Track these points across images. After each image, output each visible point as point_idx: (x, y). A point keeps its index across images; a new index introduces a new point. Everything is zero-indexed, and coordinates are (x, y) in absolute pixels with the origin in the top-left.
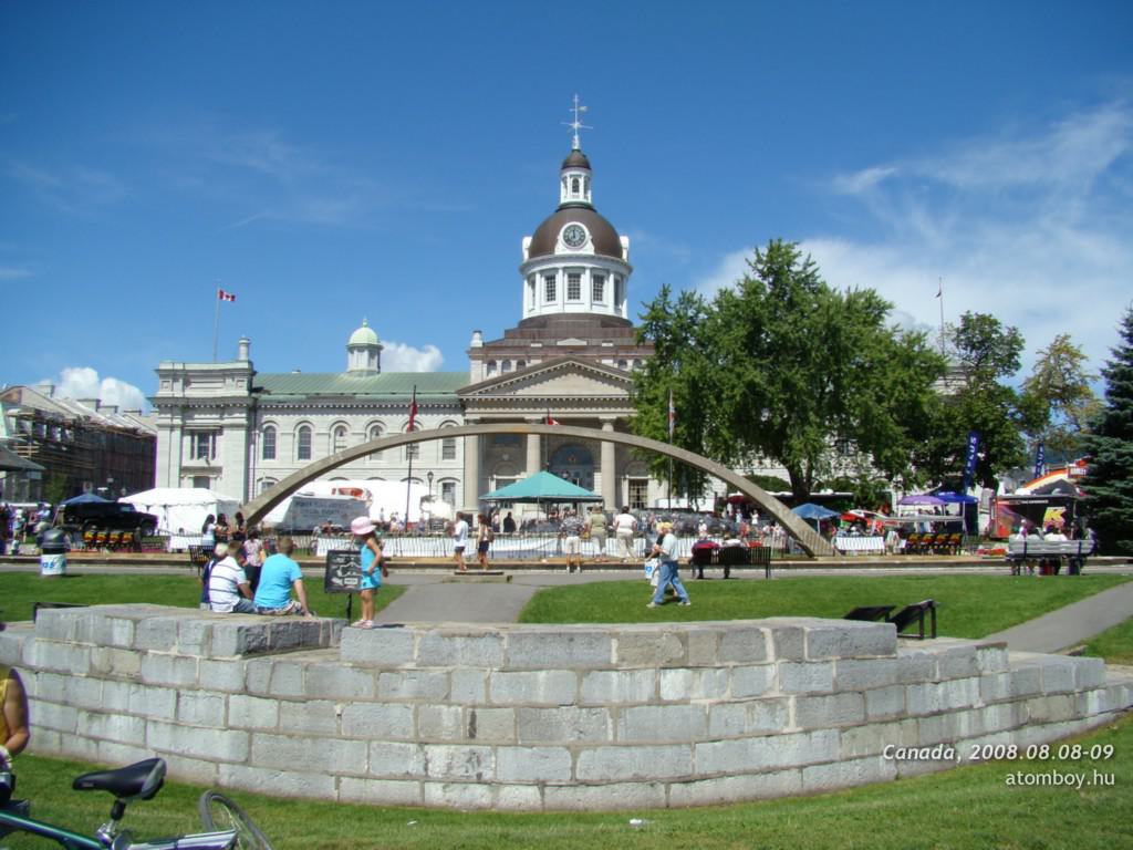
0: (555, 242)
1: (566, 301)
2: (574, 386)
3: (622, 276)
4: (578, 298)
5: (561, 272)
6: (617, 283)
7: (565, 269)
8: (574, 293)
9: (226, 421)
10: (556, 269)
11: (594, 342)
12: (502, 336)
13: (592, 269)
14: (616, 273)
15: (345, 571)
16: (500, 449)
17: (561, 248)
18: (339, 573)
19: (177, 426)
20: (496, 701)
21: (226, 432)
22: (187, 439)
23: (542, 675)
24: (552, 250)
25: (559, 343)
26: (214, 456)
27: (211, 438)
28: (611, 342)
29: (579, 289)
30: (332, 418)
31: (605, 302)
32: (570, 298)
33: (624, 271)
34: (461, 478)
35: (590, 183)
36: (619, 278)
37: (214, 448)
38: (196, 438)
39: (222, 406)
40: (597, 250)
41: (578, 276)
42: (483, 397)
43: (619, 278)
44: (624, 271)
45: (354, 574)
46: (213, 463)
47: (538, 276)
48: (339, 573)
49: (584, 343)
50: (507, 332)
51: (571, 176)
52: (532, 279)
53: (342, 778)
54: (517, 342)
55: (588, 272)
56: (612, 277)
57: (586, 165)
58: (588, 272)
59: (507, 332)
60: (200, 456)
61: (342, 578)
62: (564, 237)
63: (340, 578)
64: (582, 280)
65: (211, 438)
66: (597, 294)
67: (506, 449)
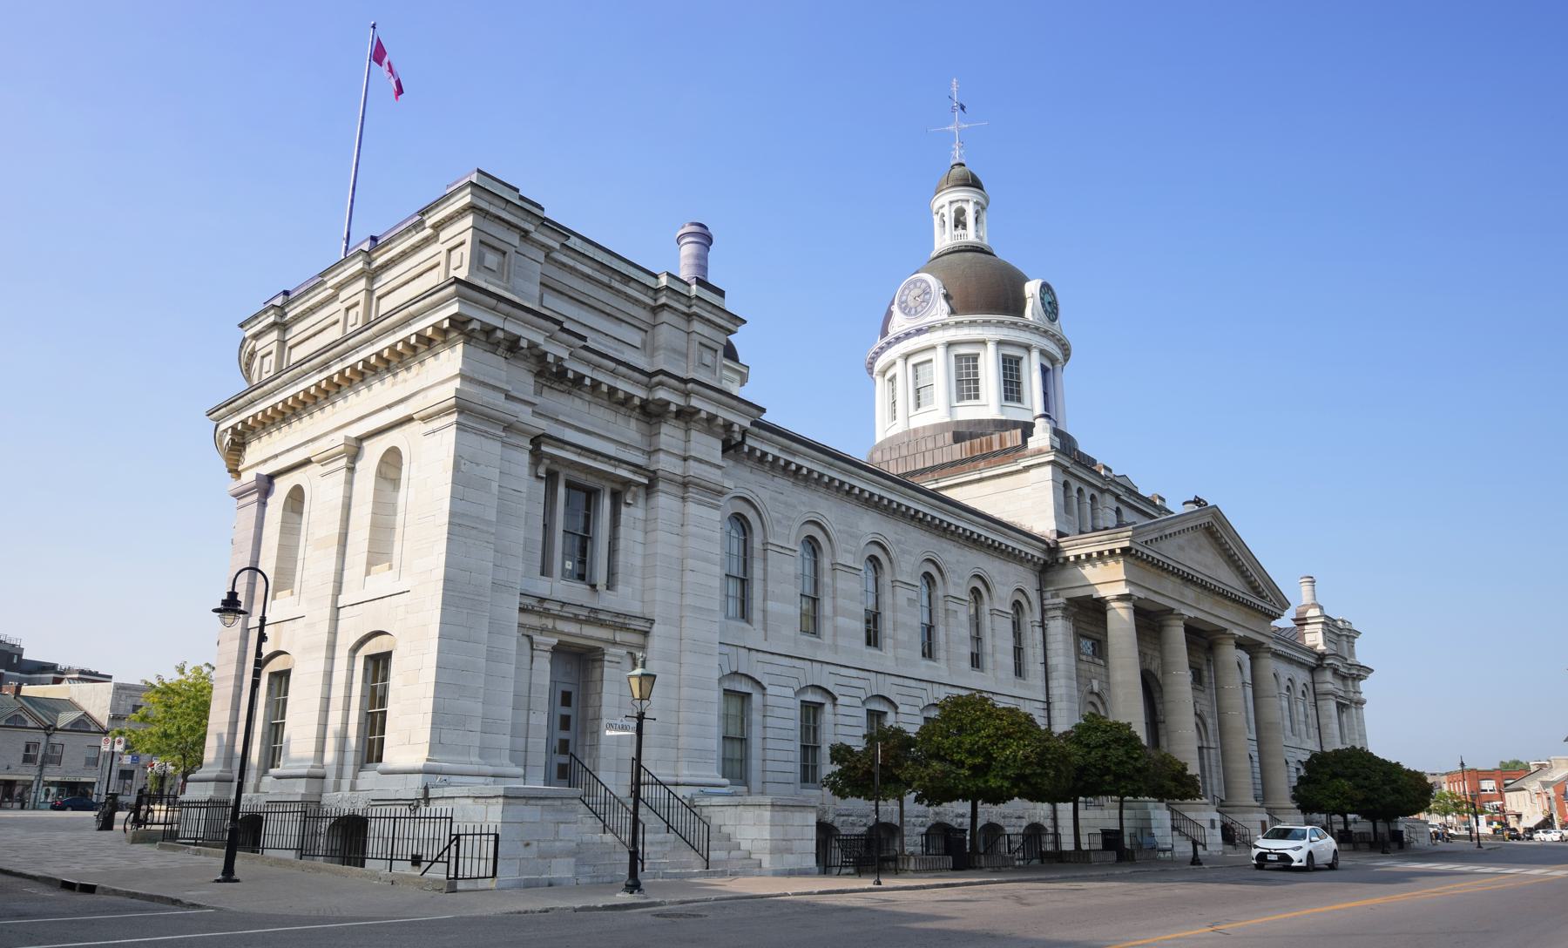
3: (1053, 360)
4: (977, 397)
5: (941, 351)
6: (1044, 370)
13: (1000, 343)
14: (1043, 353)
29: (976, 381)
31: (1027, 404)
35: (984, 217)
36: (1048, 365)
41: (975, 357)
43: (1048, 365)
47: (898, 369)
52: (889, 375)
57: (973, 183)
58: (991, 347)
64: (981, 361)
66: (1012, 389)
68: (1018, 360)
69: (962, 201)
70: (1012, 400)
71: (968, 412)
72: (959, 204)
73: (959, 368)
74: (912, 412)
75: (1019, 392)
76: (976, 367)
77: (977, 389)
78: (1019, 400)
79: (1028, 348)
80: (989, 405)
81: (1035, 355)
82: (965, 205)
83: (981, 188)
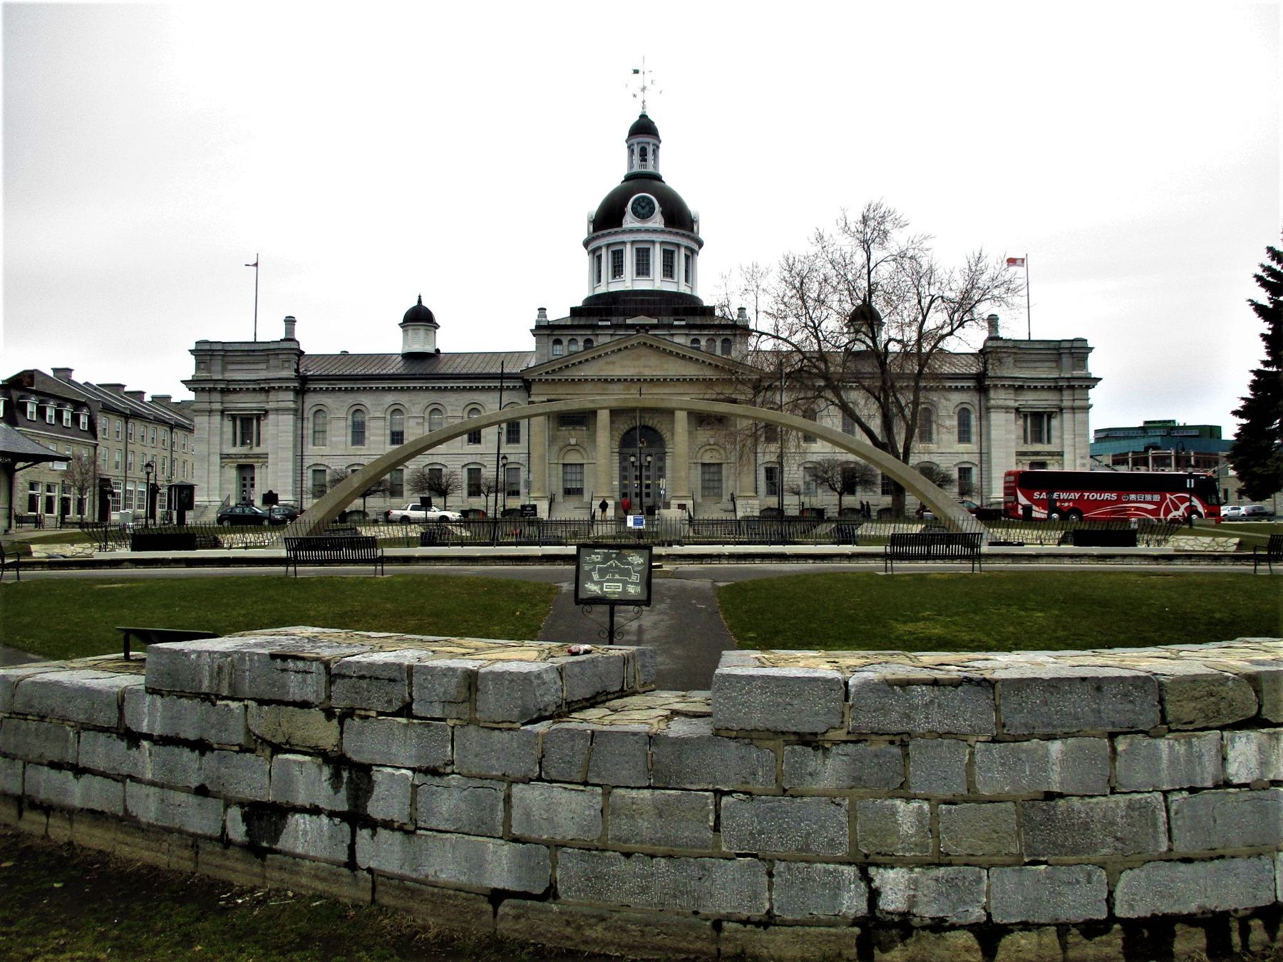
0: (623, 214)
1: (635, 278)
2: (645, 366)
4: (648, 274)
6: (687, 257)
7: (633, 242)
8: (643, 268)
9: (271, 405)
10: (624, 243)
11: (666, 320)
12: (568, 314)
13: (662, 243)
14: (687, 248)
15: (603, 573)
16: (567, 432)
17: (630, 221)
18: (596, 577)
19: (216, 411)
20: (985, 792)
21: (271, 417)
22: (228, 425)
23: (1056, 747)
24: (620, 225)
25: (629, 321)
26: (258, 444)
27: (255, 422)
28: (684, 320)
29: (648, 264)
30: (390, 399)
32: (638, 274)
33: (695, 247)
34: (526, 463)
36: (689, 254)
37: (259, 434)
38: (238, 423)
39: (264, 389)
40: (666, 224)
42: (550, 377)
43: (689, 254)
44: (695, 247)
45: (617, 577)
46: (256, 450)
47: (604, 251)
48: (596, 577)
49: (655, 321)
50: (572, 309)
51: (638, 143)
52: (598, 254)
53: (725, 924)
54: (583, 322)
55: (658, 246)
56: (683, 251)
58: (658, 246)
59: (572, 309)
60: (243, 443)
61: (600, 583)
62: (632, 209)
63: (596, 583)
65: (255, 422)
66: (668, 271)
67: (573, 432)
68: (672, 252)
69: (646, 143)
70: (667, 276)
71: (643, 285)
72: (643, 145)
73: (638, 256)
74: (610, 281)
75: (671, 272)
76: (648, 256)
77: (648, 269)
78: (672, 276)
79: (678, 246)
80: (656, 282)
81: (683, 251)
82: (647, 147)
83: (658, 136)
